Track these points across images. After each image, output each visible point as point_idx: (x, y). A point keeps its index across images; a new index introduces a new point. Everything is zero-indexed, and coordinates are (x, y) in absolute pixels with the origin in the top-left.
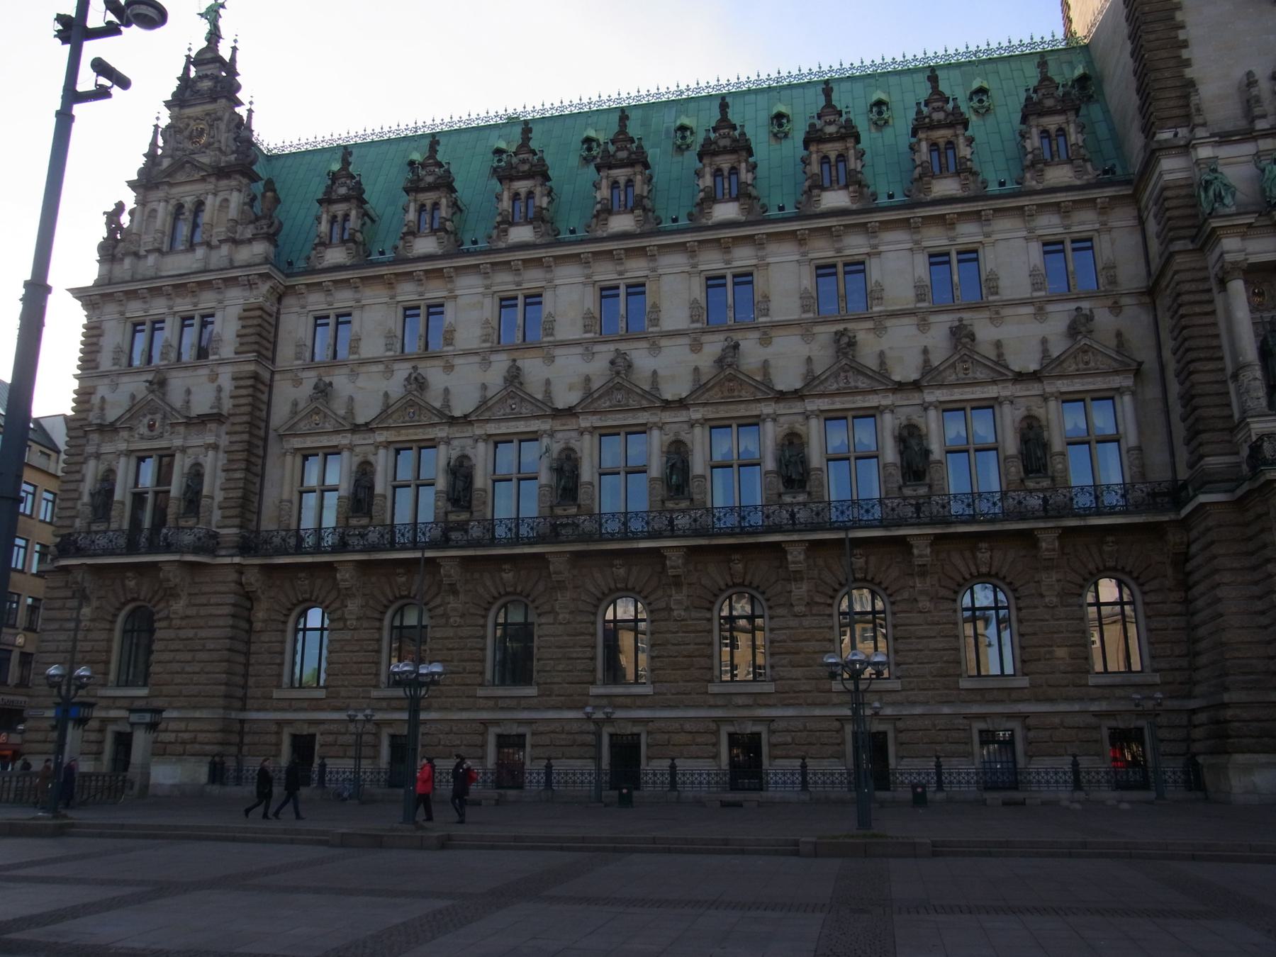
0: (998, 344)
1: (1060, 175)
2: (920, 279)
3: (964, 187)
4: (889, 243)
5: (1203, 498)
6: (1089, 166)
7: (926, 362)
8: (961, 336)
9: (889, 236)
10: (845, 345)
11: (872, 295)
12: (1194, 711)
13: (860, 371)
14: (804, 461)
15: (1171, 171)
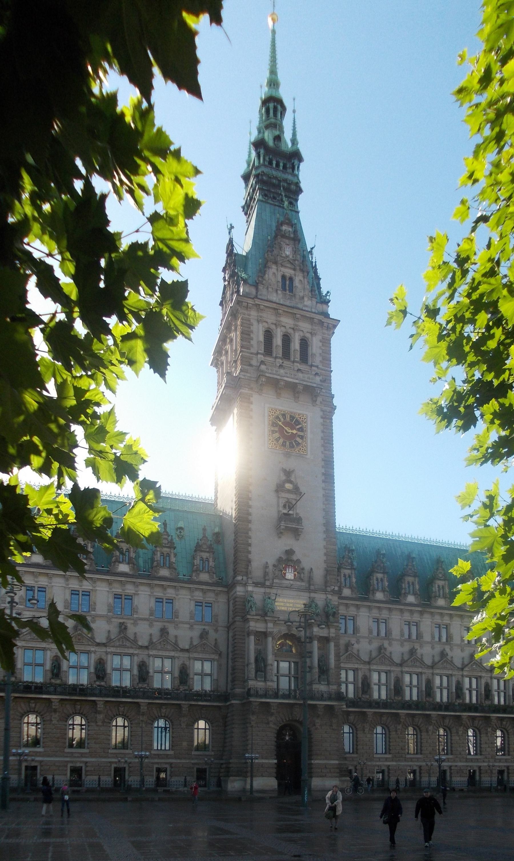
0: (176, 637)
1: (204, 577)
2: (152, 607)
3: (171, 574)
4: (142, 591)
5: (233, 702)
6: (215, 576)
7: (151, 639)
8: (164, 632)
9: (142, 588)
10: (123, 628)
11: (134, 610)
12: (222, 764)
13: (127, 639)
14: (104, 670)
15: (239, 592)
